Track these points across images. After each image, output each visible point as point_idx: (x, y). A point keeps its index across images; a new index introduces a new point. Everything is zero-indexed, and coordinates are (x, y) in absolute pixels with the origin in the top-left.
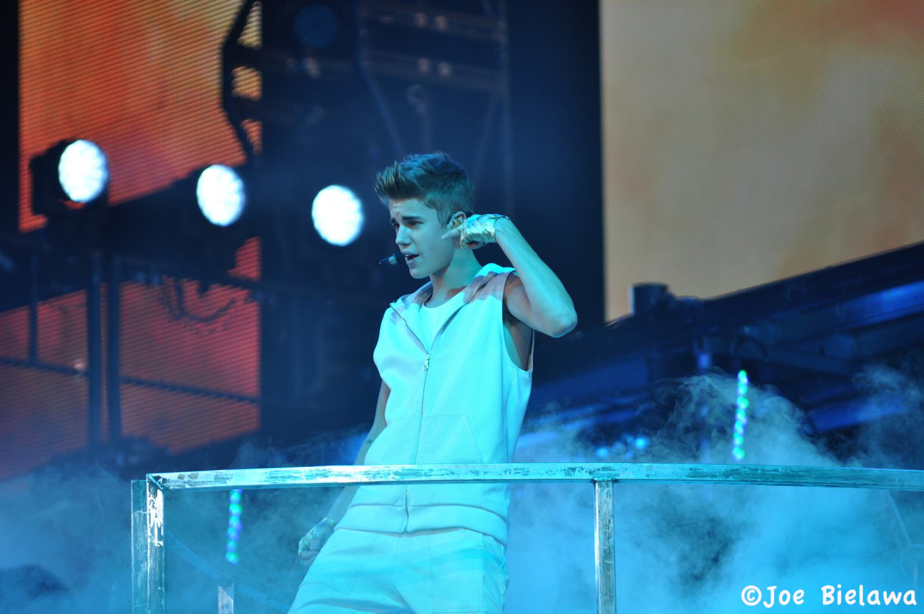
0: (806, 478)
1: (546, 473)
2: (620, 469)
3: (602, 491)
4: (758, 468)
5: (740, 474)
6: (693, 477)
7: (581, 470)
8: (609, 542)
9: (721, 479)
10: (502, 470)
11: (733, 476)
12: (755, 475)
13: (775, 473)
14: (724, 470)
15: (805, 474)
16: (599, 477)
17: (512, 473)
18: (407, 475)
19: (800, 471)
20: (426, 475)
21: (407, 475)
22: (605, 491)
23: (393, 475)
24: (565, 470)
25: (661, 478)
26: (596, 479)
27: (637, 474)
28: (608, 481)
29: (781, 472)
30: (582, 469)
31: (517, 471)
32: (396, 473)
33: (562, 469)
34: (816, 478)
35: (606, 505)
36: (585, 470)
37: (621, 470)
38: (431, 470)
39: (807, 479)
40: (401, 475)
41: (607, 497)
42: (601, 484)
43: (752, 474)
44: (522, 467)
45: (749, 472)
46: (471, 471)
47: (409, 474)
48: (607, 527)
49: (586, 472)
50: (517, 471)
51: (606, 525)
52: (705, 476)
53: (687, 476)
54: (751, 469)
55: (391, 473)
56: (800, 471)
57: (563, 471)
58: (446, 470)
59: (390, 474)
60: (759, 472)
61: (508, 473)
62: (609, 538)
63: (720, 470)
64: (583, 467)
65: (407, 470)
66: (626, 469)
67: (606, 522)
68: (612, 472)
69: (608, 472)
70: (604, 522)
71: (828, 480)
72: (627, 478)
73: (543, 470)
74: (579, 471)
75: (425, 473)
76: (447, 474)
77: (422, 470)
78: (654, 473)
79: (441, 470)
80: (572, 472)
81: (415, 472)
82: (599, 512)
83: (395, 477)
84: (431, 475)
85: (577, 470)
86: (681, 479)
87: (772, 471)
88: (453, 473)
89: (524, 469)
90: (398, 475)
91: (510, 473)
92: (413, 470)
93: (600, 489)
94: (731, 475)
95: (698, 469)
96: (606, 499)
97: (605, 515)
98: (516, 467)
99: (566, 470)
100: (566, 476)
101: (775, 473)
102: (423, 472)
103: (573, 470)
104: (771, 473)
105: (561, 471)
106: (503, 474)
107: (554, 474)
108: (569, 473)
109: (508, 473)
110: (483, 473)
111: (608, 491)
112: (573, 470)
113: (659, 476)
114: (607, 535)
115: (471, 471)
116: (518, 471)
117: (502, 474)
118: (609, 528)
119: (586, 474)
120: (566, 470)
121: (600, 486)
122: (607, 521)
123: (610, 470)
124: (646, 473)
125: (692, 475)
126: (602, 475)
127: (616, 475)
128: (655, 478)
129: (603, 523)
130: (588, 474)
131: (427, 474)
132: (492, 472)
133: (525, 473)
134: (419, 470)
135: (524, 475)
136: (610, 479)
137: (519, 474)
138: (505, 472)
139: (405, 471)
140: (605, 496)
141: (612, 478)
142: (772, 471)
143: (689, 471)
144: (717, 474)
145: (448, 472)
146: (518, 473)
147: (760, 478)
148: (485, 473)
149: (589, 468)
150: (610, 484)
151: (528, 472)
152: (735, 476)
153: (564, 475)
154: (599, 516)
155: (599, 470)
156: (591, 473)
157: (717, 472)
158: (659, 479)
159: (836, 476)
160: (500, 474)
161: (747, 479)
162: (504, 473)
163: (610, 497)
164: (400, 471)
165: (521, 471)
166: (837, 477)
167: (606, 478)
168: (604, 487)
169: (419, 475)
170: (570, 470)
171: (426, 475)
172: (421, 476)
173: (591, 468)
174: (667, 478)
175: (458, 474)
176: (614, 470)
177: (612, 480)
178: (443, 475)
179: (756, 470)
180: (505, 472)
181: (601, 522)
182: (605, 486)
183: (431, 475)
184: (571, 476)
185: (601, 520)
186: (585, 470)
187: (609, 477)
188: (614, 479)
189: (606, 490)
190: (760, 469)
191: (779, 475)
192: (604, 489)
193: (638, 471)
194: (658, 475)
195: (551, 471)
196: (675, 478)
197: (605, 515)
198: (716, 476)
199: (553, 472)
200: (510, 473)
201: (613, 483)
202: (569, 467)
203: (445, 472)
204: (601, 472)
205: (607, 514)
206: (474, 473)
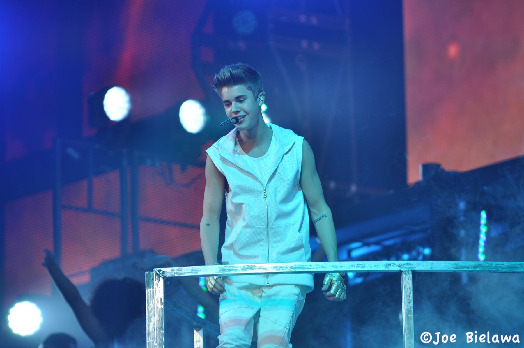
1: (375, 267)
3: (406, 276)
5: (483, 266)
6: (457, 268)
8: (410, 305)
10: (350, 266)
11: (479, 267)
12: (491, 267)
14: (474, 265)
17: (356, 267)
20: (308, 268)
23: (289, 269)
24: (385, 265)
26: (402, 270)
27: (425, 267)
28: (409, 271)
30: (395, 264)
32: (291, 267)
35: (408, 284)
36: (396, 265)
37: (416, 265)
38: (310, 266)
40: (294, 269)
41: (409, 280)
43: (490, 267)
45: (488, 266)
46: (333, 266)
48: (409, 297)
49: (397, 266)
50: (358, 266)
52: (463, 268)
53: (453, 268)
54: (489, 264)
55: (289, 267)
58: (319, 266)
61: (353, 267)
62: (410, 303)
65: (297, 265)
66: (419, 264)
69: (409, 266)
74: (393, 265)
75: (307, 267)
76: (320, 268)
77: (306, 266)
78: (434, 266)
79: (316, 265)
80: (389, 266)
81: (302, 267)
82: (404, 288)
84: (311, 268)
85: (392, 265)
88: (323, 267)
89: (362, 264)
91: (355, 267)
92: (301, 265)
93: (404, 275)
94: (478, 267)
97: (408, 289)
100: (386, 268)
103: (390, 265)
106: (351, 267)
108: (387, 267)
109: (353, 267)
110: (340, 267)
111: (409, 276)
112: (390, 265)
113: (438, 268)
115: (333, 266)
116: (359, 266)
118: (410, 297)
121: (405, 274)
122: (409, 293)
123: (410, 265)
124: (430, 267)
125: (456, 267)
127: (413, 268)
129: (407, 295)
130: (398, 267)
131: (309, 268)
132: (344, 266)
133: (363, 267)
134: (304, 266)
135: (362, 268)
136: (410, 270)
137: (359, 267)
138: (352, 266)
139: (296, 266)
140: (408, 279)
143: (454, 265)
144: (470, 267)
145: (320, 266)
146: (359, 267)
148: (341, 267)
149: (398, 264)
151: (365, 266)
155: (404, 265)
156: (399, 266)
160: (349, 268)
161: (486, 269)
164: (294, 266)
165: (361, 266)
167: (408, 269)
169: (304, 268)
171: (308, 268)
172: (305, 269)
176: (412, 265)
177: (411, 270)
178: (317, 268)
180: (352, 266)
181: (405, 294)
182: (408, 274)
183: (311, 268)
186: (396, 265)
188: (412, 270)
189: (408, 276)
192: (407, 275)
194: (437, 267)
197: (408, 289)
198: (469, 268)
199: (378, 266)
200: (355, 267)
202: (387, 263)
204: (405, 266)
205: (409, 289)
206: (334, 267)
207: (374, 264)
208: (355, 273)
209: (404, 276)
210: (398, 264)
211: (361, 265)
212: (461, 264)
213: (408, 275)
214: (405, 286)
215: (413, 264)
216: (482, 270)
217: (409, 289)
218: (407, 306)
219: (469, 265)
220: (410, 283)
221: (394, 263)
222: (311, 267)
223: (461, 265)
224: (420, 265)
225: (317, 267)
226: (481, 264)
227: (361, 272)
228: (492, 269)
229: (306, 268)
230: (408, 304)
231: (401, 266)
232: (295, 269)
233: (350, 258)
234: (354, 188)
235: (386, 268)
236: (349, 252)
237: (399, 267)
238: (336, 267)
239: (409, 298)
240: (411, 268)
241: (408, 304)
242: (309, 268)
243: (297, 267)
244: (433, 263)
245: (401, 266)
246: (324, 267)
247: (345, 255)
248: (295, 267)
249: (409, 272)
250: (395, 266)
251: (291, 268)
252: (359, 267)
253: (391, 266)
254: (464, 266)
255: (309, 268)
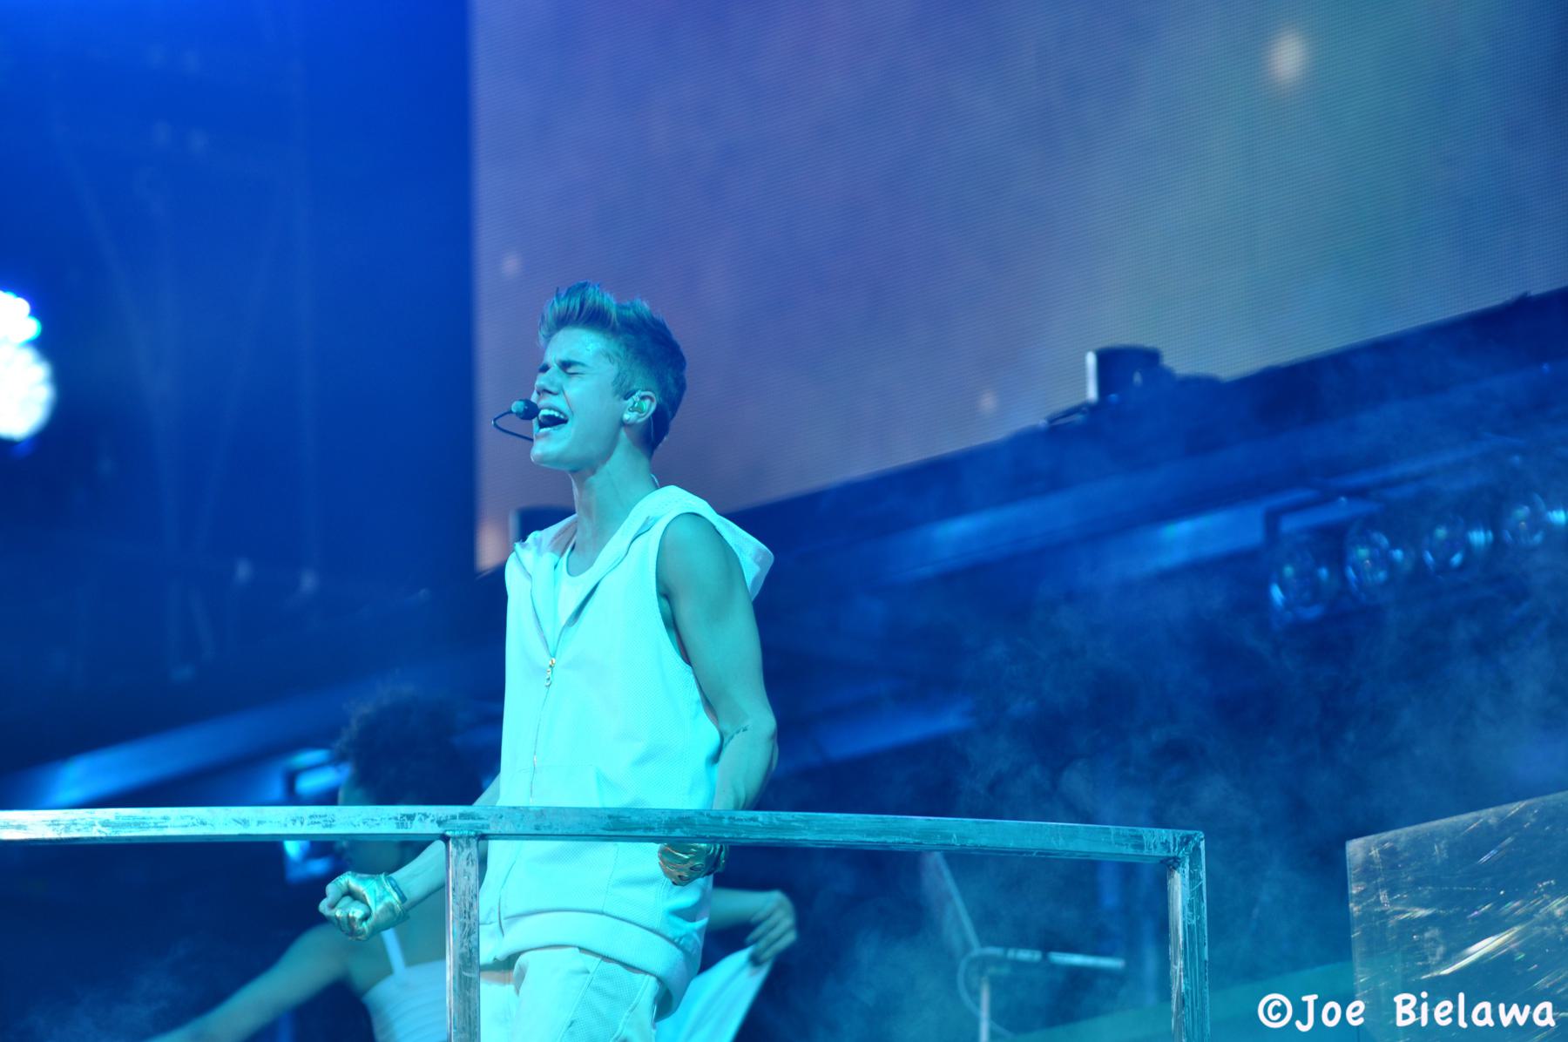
0: (805, 832)
1: (364, 823)
2: (489, 817)
3: (458, 853)
4: (724, 815)
5: (695, 825)
6: (614, 830)
7: (423, 818)
8: (470, 941)
9: (661, 834)
10: (288, 819)
11: (682, 828)
12: (718, 826)
13: (752, 823)
14: (667, 819)
15: (802, 825)
16: (454, 831)
17: (306, 822)
18: (123, 825)
19: (794, 821)
20: (157, 827)
21: (123, 825)
22: (463, 854)
23: (99, 827)
24: (396, 819)
25: (560, 832)
26: (448, 833)
27: (519, 826)
28: (469, 837)
29: (762, 823)
30: (426, 816)
31: (313, 820)
32: (106, 824)
33: (390, 816)
34: (820, 832)
35: (466, 877)
36: (431, 818)
37: (491, 819)
38: (165, 818)
39: (806, 835)
40: (113, 827)
41: (468, 864)
42: (457, 842)
43: (714, 826)
44: (324, 814)
45: (708, 823)
46: (235, 820)
47: (129, 825)
48: (467, 916)
49: (432, 821)
50: (313, 820)
51: (465, 912)
52: (635, 829)
53: (604, 829)
54: (712, 817)
55: (97, 823)
56: (794, 821)
57: (394, 821)
58: (192, 818)
59: (94, 825)
60: (726, 821)
61: (298, 823)
62: (469, 935)
63: (659, 818)
64: (428, 814)
65: (124, 818)
66: (501, 817)
67: (465, 905)
68: (475, 822)
69: (471, 821)
70: (462, 906)
71: (841, 836)
72: (503, 832)
73: (358, 820)
74: (421, 819)
75: (155, 823)
76: (194, 825)
77: (151, 818)
78: (547, 824)
79: (182, 818)
80: (409, 823)
81: (138, 821)
82: (454, 889)
83: (104, 829)
84: (167, 827)
85: (417, 818)
86: (594, 833)
87: (746, 820)
88: (203, 824)
89: (325, 816)
90: (108, 826)
91: (302, 823)
92: (134, 818)
93: (455, 850)
94: (677, 828)
95: (621, 817)
96: (466, 867)
97: (464, 895)
98: (312, 813)
99: (399, 818)
100: (398, 827)
101: (752, 823)
102: (152, 821)
103: (411, 817)
104: (745, 823)
105: (390, 819)
106: (290, 824)
107: (378, 824)
108: (402, 824)
109: (298, 823)
110: (256, 823)
111: (470, 854)
112: (411, 817)
113: (557, 829)
114: (467, 929)
115: (235, 820)
116: (317, 820)
117: (288, 825)
118: (469, 917)
119: (431, 825)
120: (399, 818)
121: (456, 845)
122: (467, 905)
123: (473, 818)
124: (535, 823)
125: (612, 827)
126: (458, 827)
127: (483, 827)
128: (549, 832)
129: (461, 911)
130: (436, 825)
131: (159, 825)
132: (271, 822)
133: (329, 823)
134: (144, 818)
135: (327, 826)
136: (473, 833)
137: (316, 825)
138: (294, 821)
139: (120, 820)
140: (465, 863)
141: (476, 832)
142: (746, 820)
143: (608, 821)
144: (656, 825)
145: (194, 821)
146: (315, 823)
147: (727, 832)
148: (259, 823)
149: (437, 814)
150: (473, 842)
151: (333, 821)
152: (685, 829)
153: (395, 826)
154: (453, 896)
155: (454, 817)
156: (440, 823)
157: (654, 822)
158: (556, 833)
159: (854, 829)
160: (286, 825)
161: (704, 834)
162: (291, 822)
163: (473, 864)
164: (112, 819)
165: (321, 820)
166: (857, 830)
167: (466, 832)
168: (462, 848)
169: (145, 825)
170: (405, 818)
171: (156, 826)
172: (149, 827)
173: (440, 815)
174: (570, 832)
175: (212, 825)
176: (480, 819)
177: (476, 835)
178: (186, 826)
179: (721, 818)
180: (294, 821)
181: (456, 907)
182: (465, 845)
183: (167, 827)
184: (407, 828)
185: (457, 904)
186: (431, 818)
187: (471, 831)
188: (479, 833)
189: (466, 852)
190: (727, 817)
191: (758, 827)
192: (463, 851)
193: (522, 819)
194: (555, 827)
195: (372, 820)
196: (583, 833)
197: (464, 895)
198: (652, 829)
199: (375, 822)
200: (302, 823)
201: (478, 840)
202: (403, 812)
203: (191, 821)
204: (459, 822)
205: (467, 893)
206: (238, 822)
207: (364, 816)
208: (305, 843)
209: (455, 854)
210: (437, 814)
211: (323, 819)
212: (629, 817)
213: (465, 850)
214: (455, 884)
215: (483, 816)
216: (689, 835)
217: (467, 893)
218: (459, 944)
219: (651, 819)
220: (470, 874)
221: (423, 812)
222: (168, 823)
223: (628, 821)
224: (503, 818)
225: (186, 823)
226: (689, 818)
227: (322, 839)
228: (720, 832)
229: (153, 825)
230: (464, 938)
231: (446, 820)
232: (115, 830)
233: (292, 797)
234: (309, 582)
235: (398, 827)
236: (291, 778)
237: (439, 826)
238: (245, 822)
239: (467, 922)
240: (477, 827)
241: (464, 938)
242: (162, 827)
243: (125, 821)
244: (543, 814)
245: (446, 820)
246: (209, 822)
247: (277, 788)
248: (117, 821)
249: (470, 840)
250: (429, 820)
251: (103, 826)
252: (315, 823)
253: (414, 822)
254: (637, 823)
255: (162, 827)
